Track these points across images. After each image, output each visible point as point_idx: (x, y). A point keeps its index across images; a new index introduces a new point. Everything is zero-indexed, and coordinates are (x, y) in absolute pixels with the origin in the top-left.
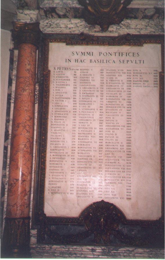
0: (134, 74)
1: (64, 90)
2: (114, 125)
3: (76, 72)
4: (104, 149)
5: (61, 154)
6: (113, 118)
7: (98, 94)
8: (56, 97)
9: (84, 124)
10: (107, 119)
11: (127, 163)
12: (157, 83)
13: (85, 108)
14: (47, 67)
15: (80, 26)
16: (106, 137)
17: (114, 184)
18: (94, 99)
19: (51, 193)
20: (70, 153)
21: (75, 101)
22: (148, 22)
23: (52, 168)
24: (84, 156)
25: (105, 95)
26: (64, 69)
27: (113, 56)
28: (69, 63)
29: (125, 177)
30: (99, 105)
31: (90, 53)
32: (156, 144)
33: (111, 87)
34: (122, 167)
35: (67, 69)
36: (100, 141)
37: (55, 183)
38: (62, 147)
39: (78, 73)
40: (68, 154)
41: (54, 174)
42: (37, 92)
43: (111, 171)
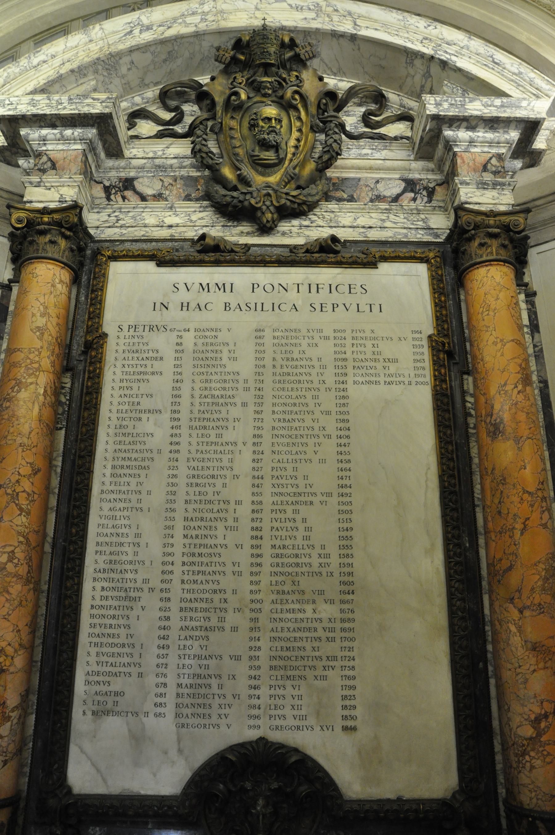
0: (355, 342)
1: (144, 388)
2: (299, 490)
3: (181, 337)
4: (267, 569)
5: (129, 585)
6: (295, 469)
7: (249, 397)
8: (121, 407)
9: (202, 489)
10: (275, 473)
11: (342, 611)
12: (422, 365)
13: (205, 439)
14: (100, 325)
15: (200, 219)
16: (272, 528)
17: (302, 683)
18: (235, 412)
19: (89, 713)
20: (156, 583)
21: (175, 419)
22: (386, 209)
23: (97, 631)
24: (204, 591)
25: (268, 400)
26: (147, 328)
27: (292, 295)
28: (162, 315)
29: (335, 658)
30: (251, 431)
31: (224, 284)
32: (433, 545)
33: (287, 378)
34: (326, 624)
35: (155, 329)
36: (254, 542)
37: (107, 679)
38: (131, 562)
39: (189, 339)
40: (151, 585)
41: (105, 650)
42: (65, 396)
43: (289, 639)
